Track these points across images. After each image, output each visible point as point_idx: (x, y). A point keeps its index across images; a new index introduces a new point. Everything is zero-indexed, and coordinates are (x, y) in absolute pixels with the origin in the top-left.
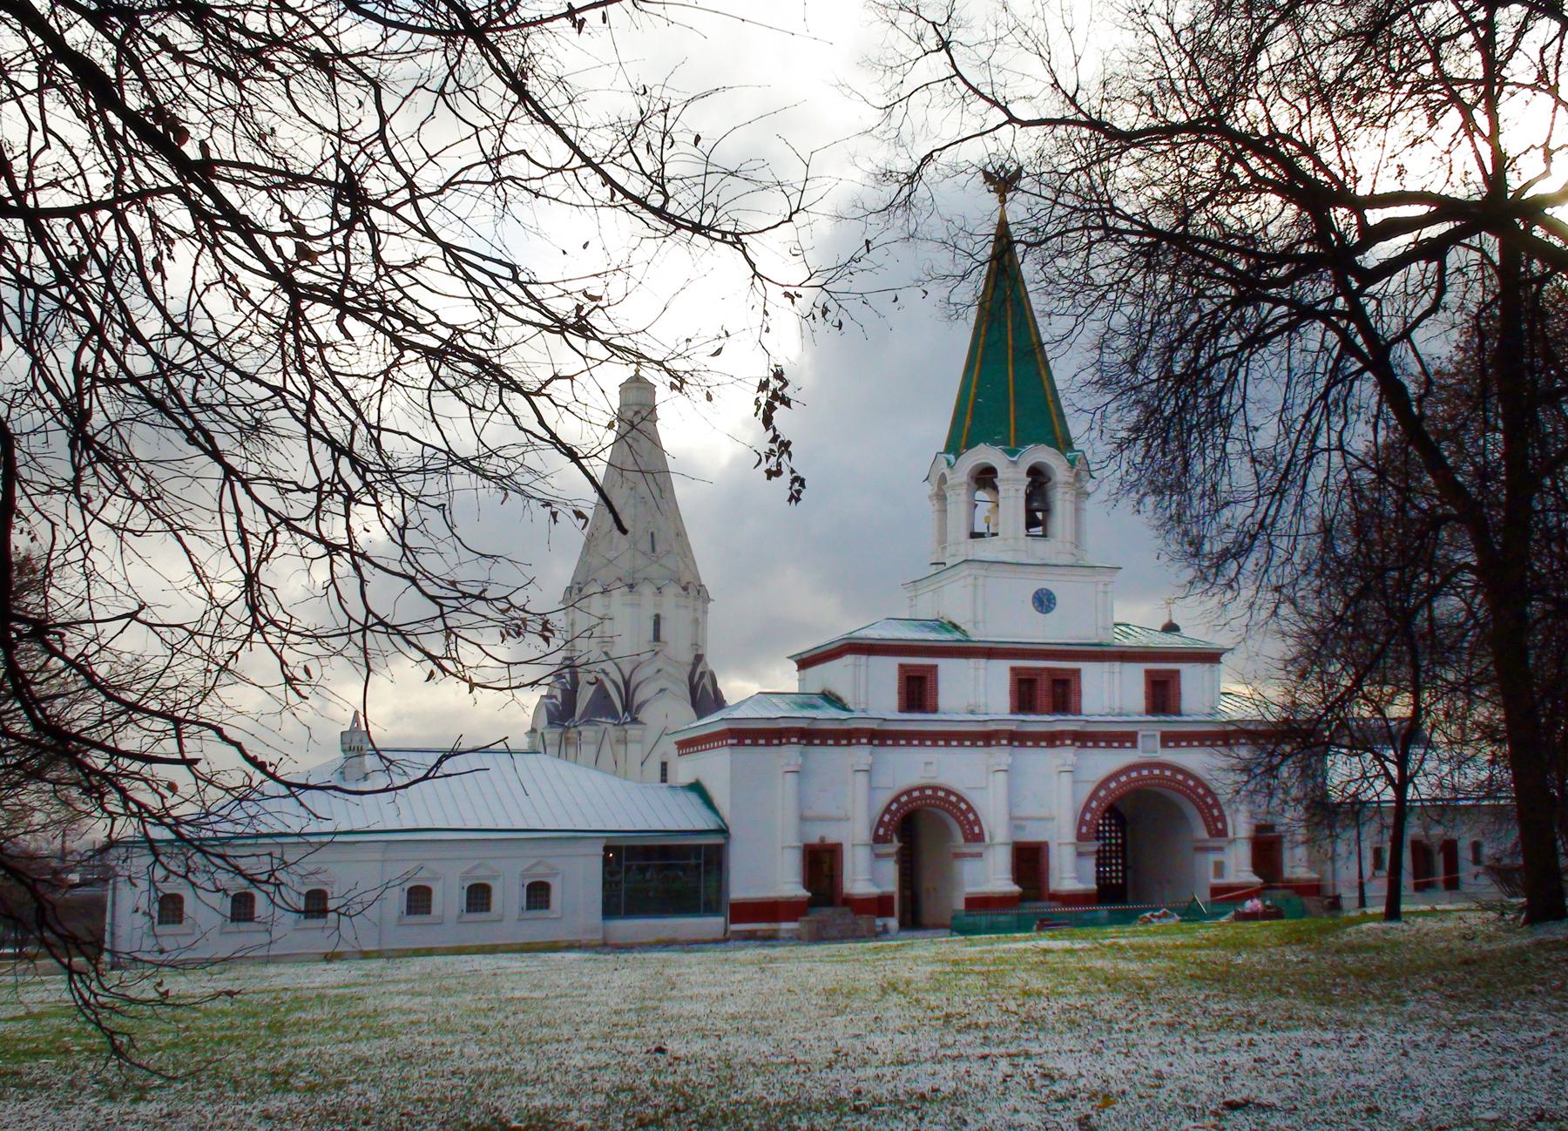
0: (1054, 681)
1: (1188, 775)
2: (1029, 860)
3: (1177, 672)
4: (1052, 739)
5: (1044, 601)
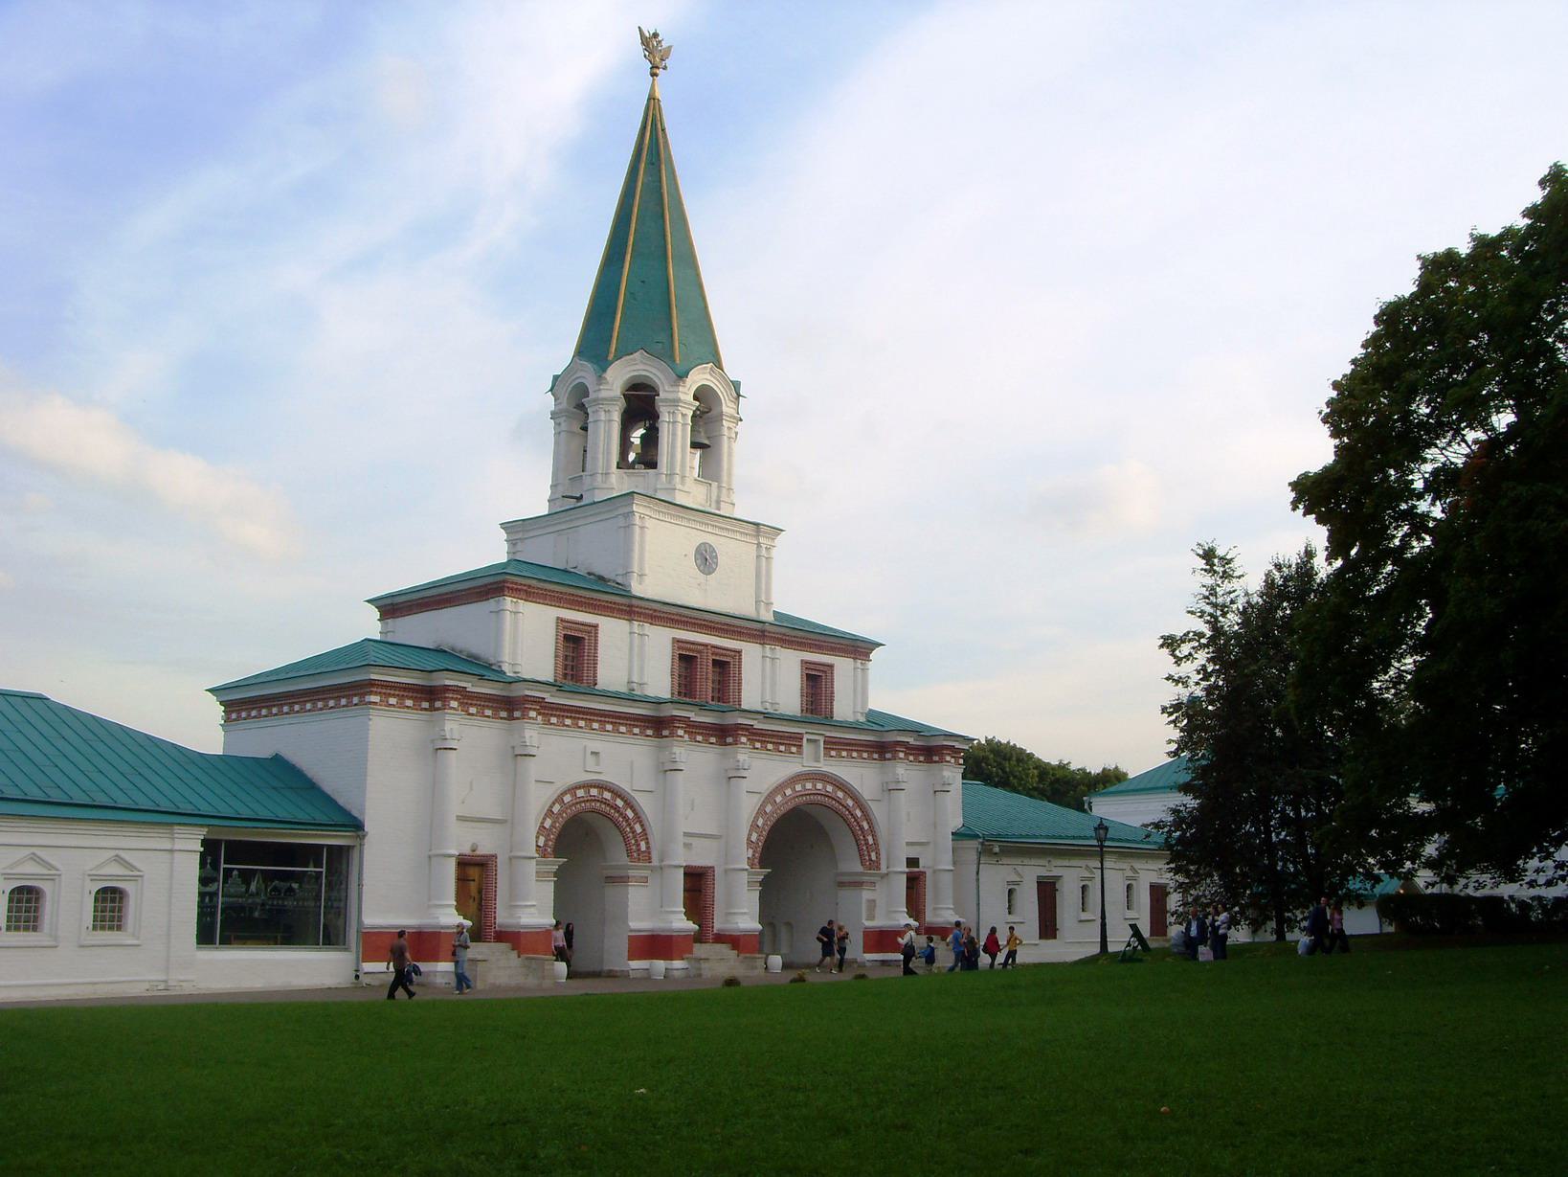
4: (723, 734)
5: (706, 559)
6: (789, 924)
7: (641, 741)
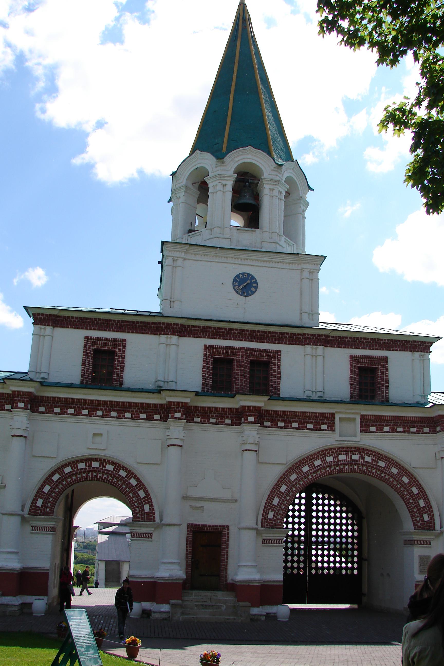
0: (252, 363)
1: (391, 462)
3: (386, 359)
5: (245, 285)
6: (388, 575)
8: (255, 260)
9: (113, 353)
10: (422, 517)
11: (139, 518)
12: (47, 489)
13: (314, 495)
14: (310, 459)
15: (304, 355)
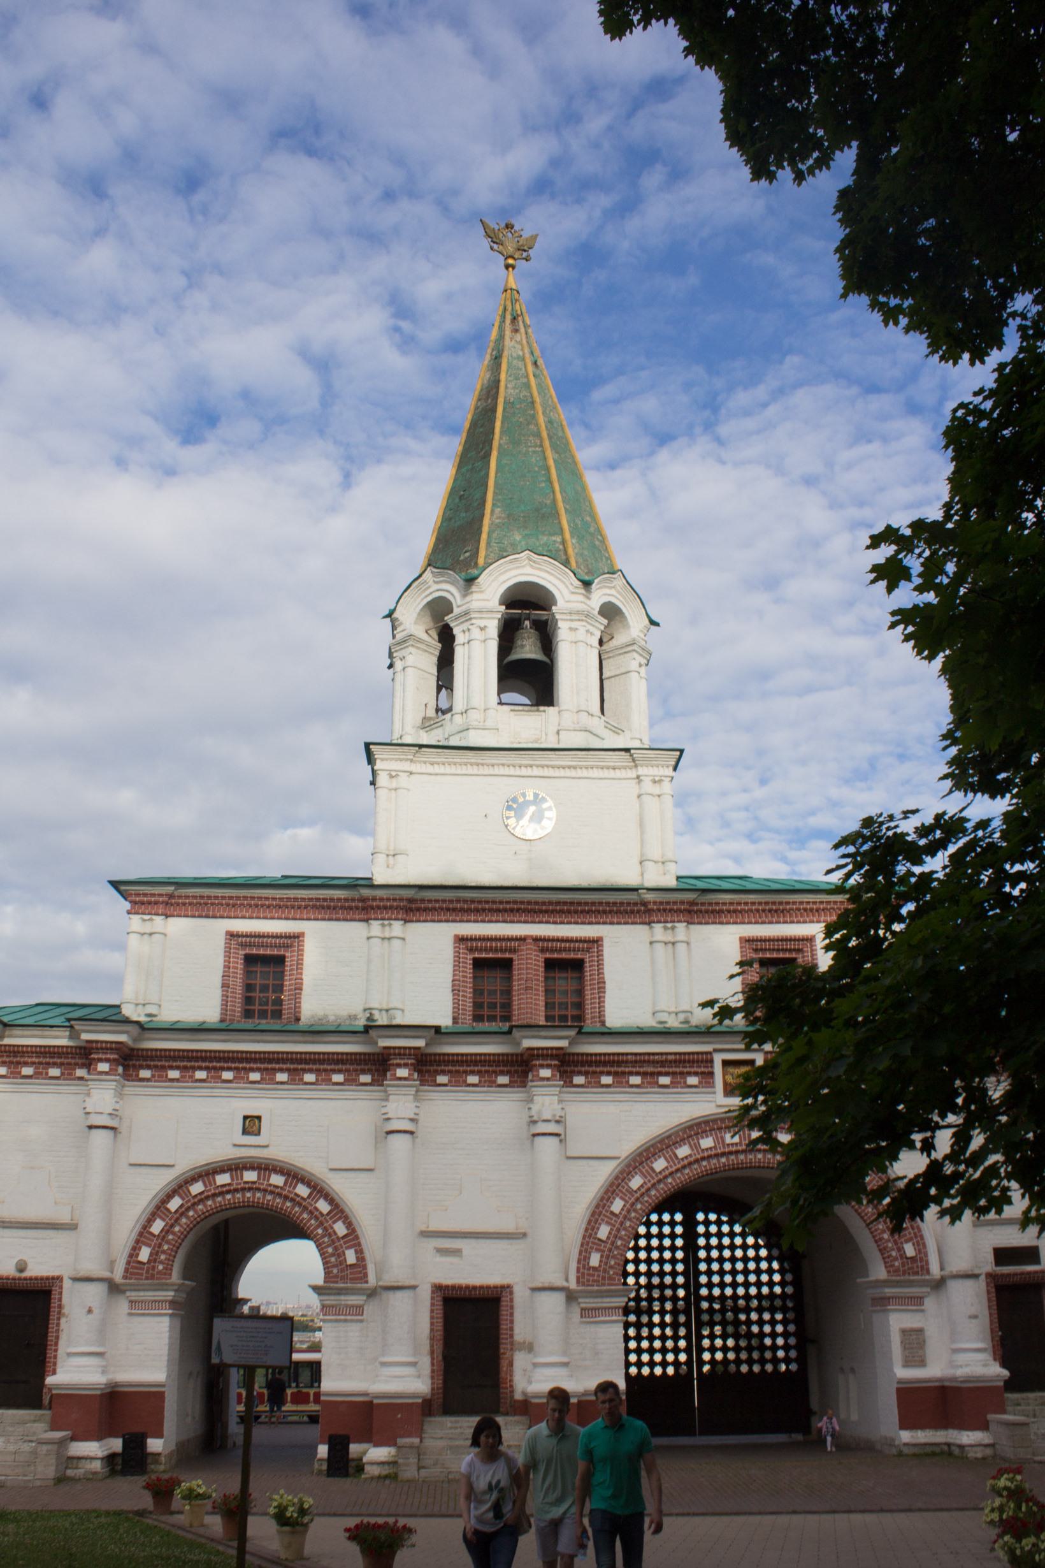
2: (472, 1327)
4: (519, 1068)
6: (853, 1370)
7: (351, 1092)
8: (548, 766)
9: (280, 960)
10: (900, 1250)
11: (336, 1276)
12: (157, 1227)
13: (700, 1217)
14: (668, 1146)
15: (651, 943)
